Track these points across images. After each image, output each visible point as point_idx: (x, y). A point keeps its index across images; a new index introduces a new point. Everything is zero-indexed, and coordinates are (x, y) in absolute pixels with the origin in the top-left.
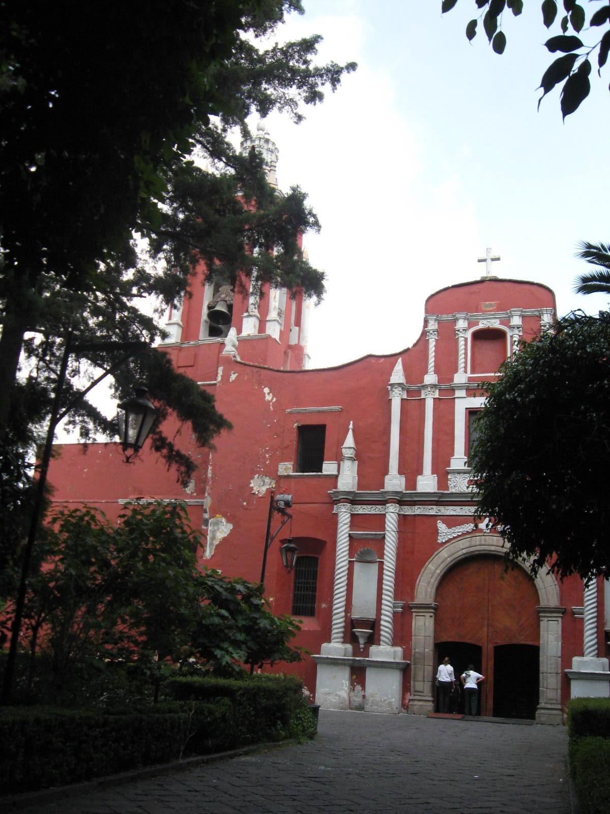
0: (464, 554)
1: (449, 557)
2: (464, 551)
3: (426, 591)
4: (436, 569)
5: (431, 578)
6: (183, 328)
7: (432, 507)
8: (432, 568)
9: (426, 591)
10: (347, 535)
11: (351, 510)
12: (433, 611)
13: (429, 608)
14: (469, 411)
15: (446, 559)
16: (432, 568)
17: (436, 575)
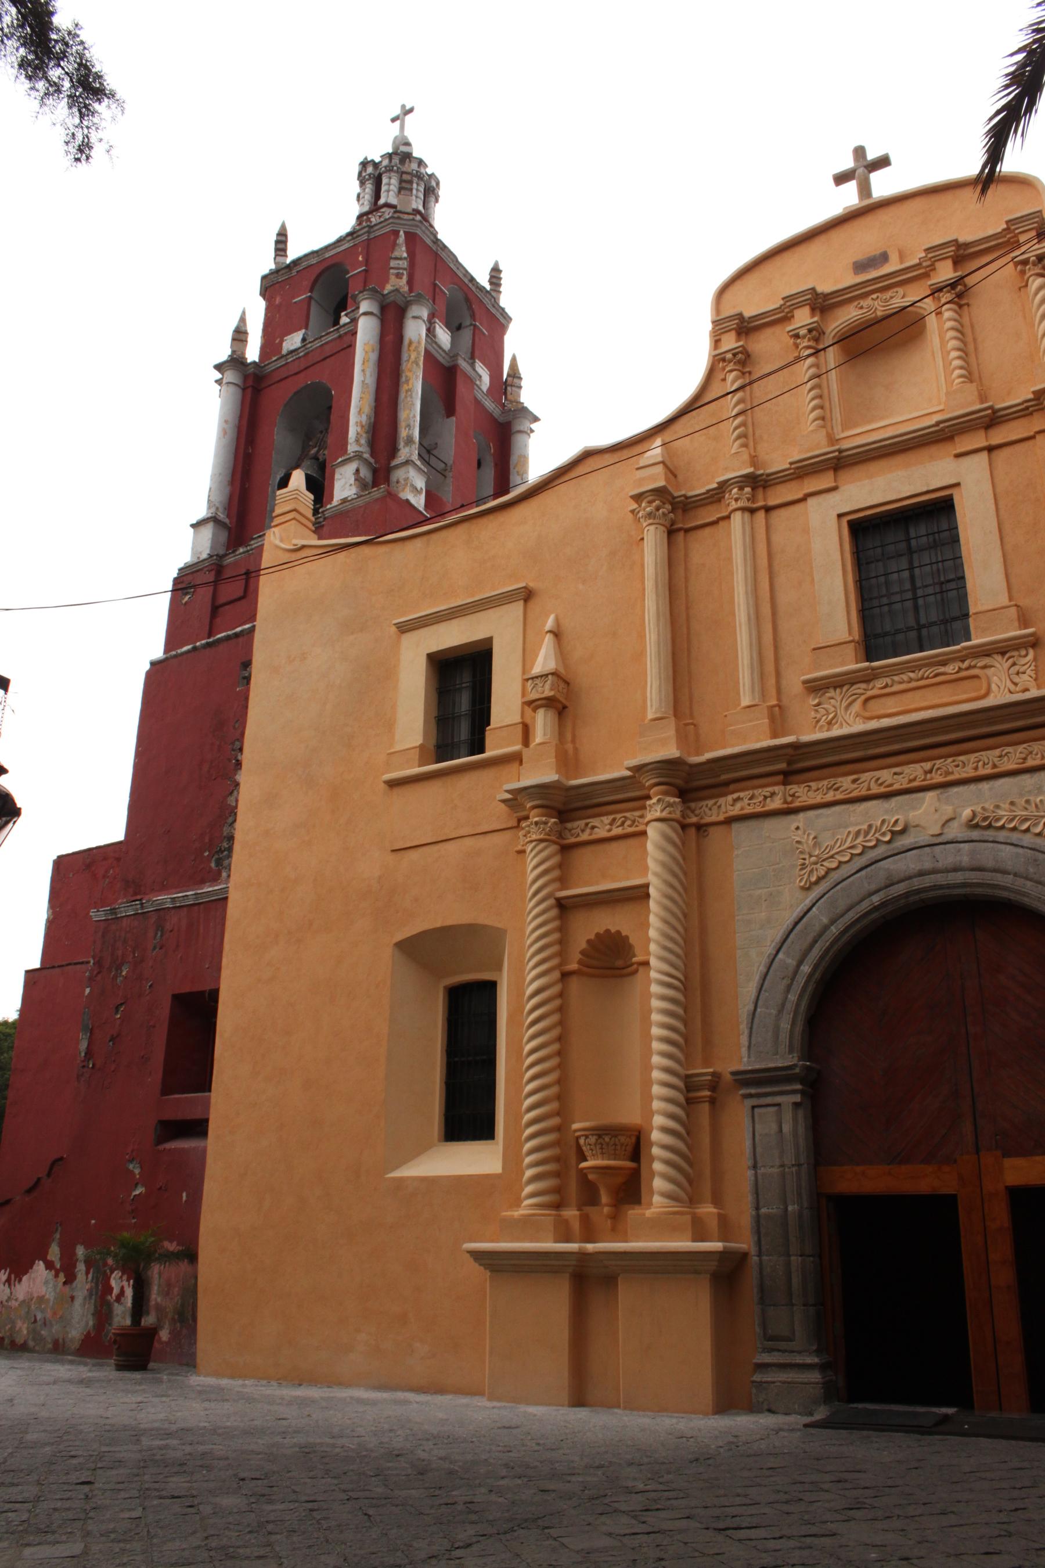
0: (876, 909)
1: (833, 922)
2: (876, 899)
3: (777, 1030)
4: (800, 963)
5: (789, 988)
6: (230, 530)
7: (770, 789)
8: (789, 961)
9: (777, 1030)
10: (551, 902)
11: (561, 836)
12: (799, 1087)
13: (789, 1079)
14: (851, 523)
15: (826, 928)
16: (789, 961)
17: (801, 980)
